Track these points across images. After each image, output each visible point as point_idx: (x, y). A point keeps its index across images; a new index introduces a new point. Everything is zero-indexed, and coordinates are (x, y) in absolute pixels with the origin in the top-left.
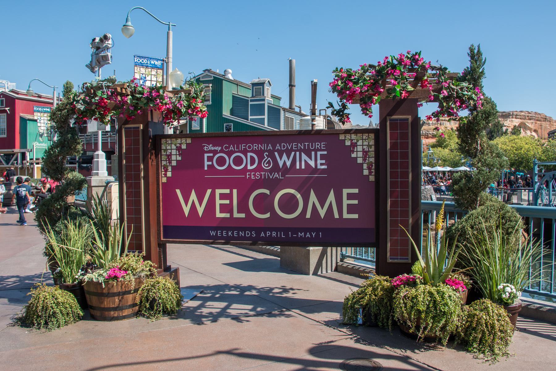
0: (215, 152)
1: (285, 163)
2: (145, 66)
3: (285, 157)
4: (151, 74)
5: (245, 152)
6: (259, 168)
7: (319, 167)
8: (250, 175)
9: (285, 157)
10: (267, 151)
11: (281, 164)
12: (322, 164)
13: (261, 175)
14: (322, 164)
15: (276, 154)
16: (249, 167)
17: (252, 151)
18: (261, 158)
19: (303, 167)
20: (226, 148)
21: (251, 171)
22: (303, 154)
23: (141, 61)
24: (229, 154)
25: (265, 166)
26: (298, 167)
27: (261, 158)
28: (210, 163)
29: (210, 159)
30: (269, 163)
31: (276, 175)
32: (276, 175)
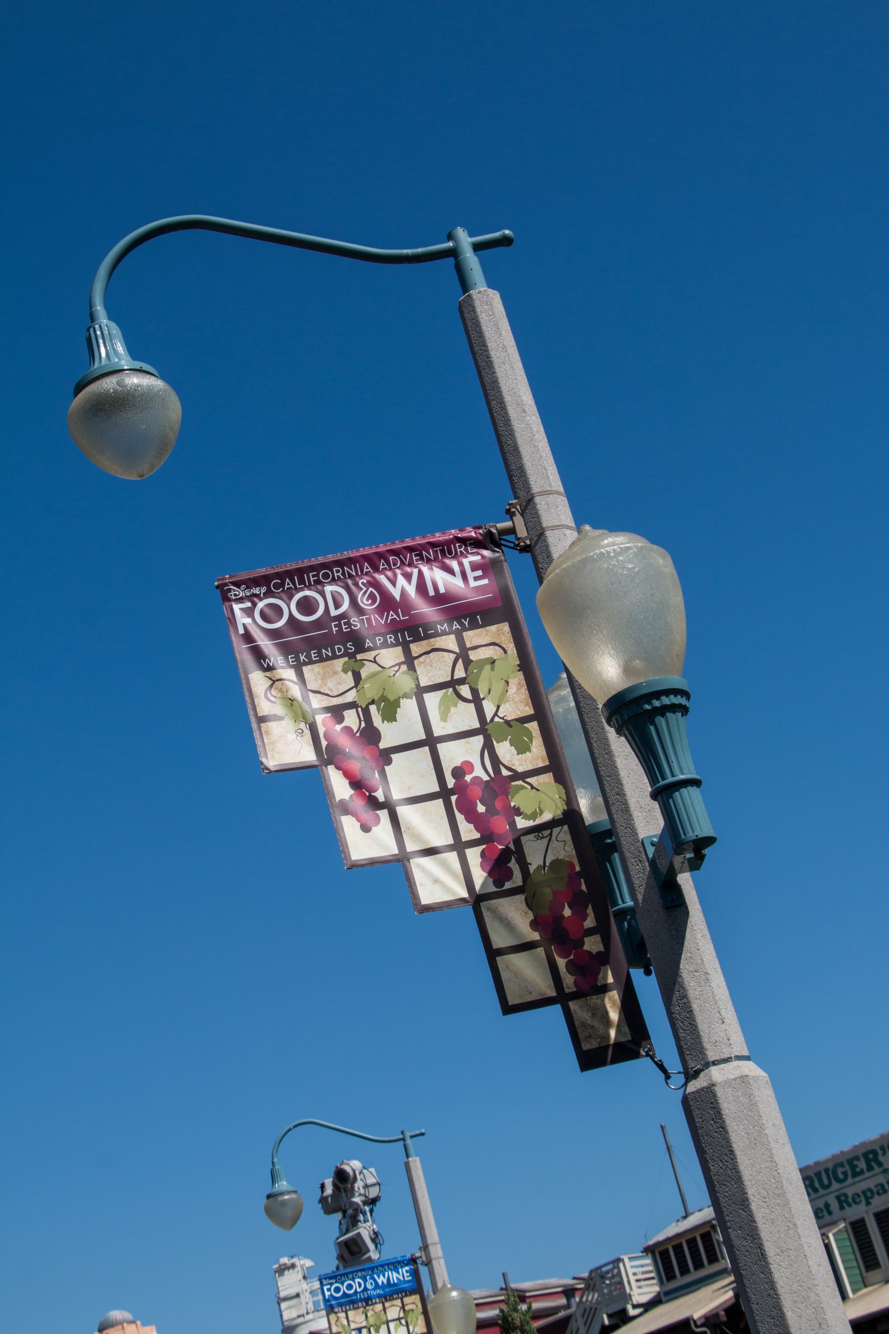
0: (331, 1284)
1: (383, 1282)
2: (361, 1300)
3: (381, 1277)
4: (384, 1319)
5: (353, 1280)
6: (365, 1289)
7: (406, 1279)
8: (360, 1295)
9: (381, 1277)
10: (369, 1275)
11: (380, 1283)
12: (408, 1277)
13: (368, 1294)
14: (408, 1277)
15: (375, 1276)
16: (359, 1290)
17: (359, 1277)
18: (365, 1280)
19: (396, 1281)
20: (339, 1279)
21: (360, 1292)
22: (394, 1273)
23: (343, 1288)
24: (342, 1283)
25: (369, 1286)
26: (392, 1282)
27: (365, 1280)
28: (329, 1293)
29: (329, 1290)
30: (371, 1284)
31: (378, 1291)
32: (378, 1291)
